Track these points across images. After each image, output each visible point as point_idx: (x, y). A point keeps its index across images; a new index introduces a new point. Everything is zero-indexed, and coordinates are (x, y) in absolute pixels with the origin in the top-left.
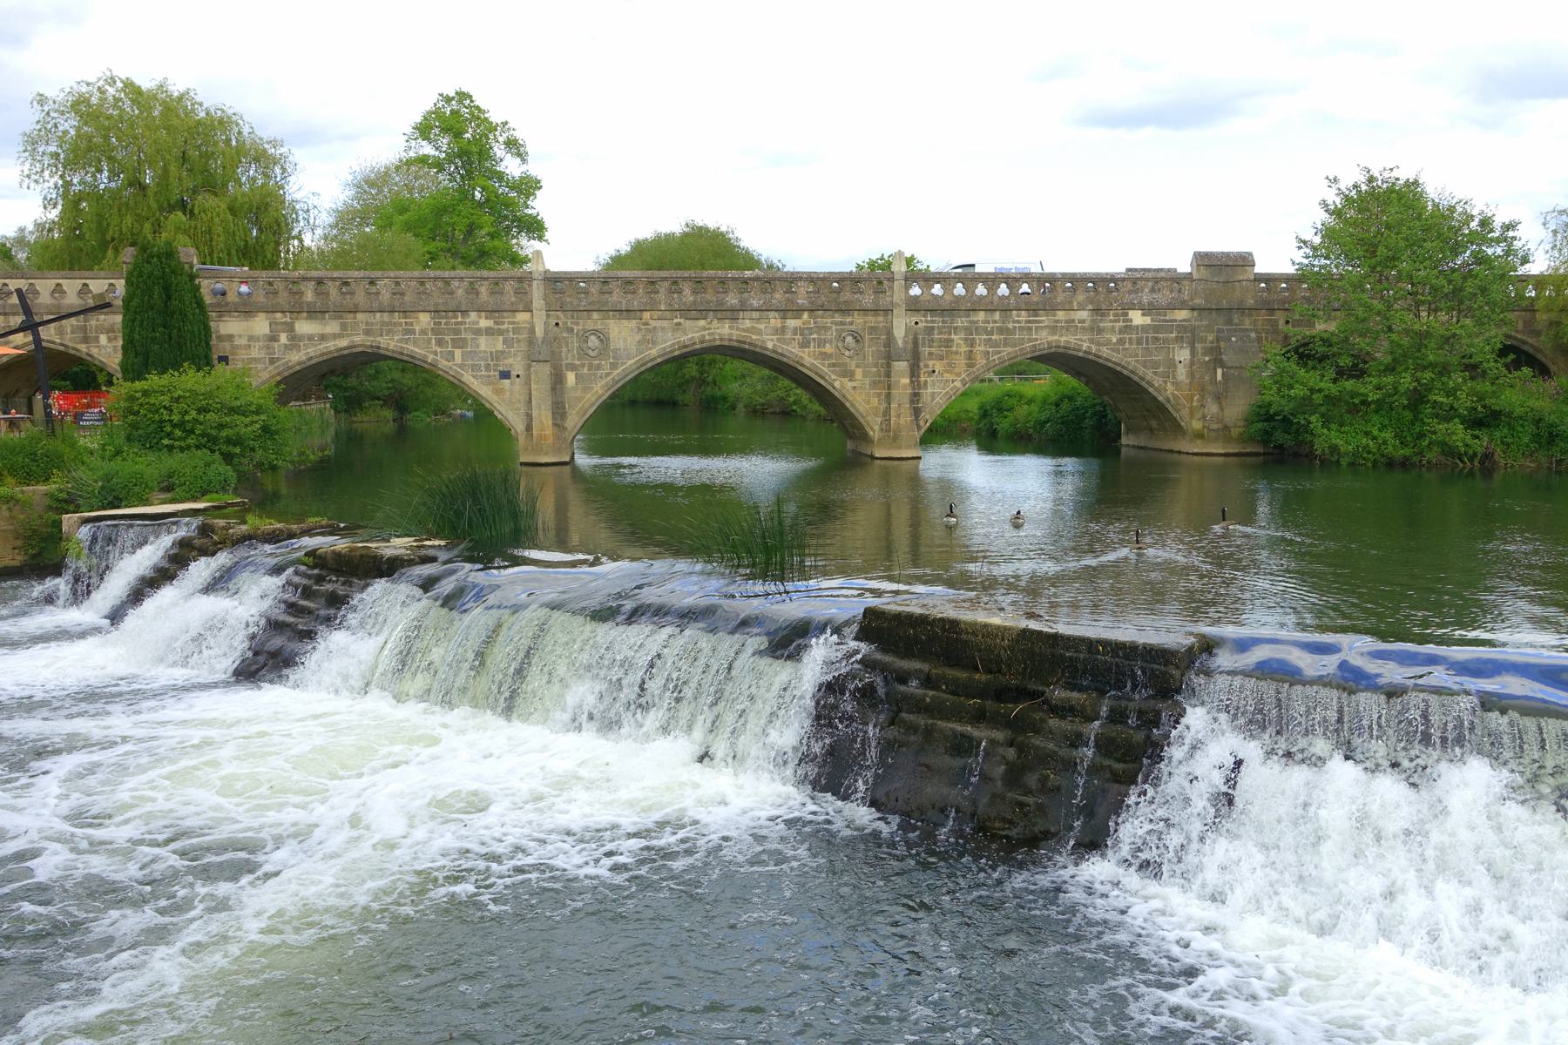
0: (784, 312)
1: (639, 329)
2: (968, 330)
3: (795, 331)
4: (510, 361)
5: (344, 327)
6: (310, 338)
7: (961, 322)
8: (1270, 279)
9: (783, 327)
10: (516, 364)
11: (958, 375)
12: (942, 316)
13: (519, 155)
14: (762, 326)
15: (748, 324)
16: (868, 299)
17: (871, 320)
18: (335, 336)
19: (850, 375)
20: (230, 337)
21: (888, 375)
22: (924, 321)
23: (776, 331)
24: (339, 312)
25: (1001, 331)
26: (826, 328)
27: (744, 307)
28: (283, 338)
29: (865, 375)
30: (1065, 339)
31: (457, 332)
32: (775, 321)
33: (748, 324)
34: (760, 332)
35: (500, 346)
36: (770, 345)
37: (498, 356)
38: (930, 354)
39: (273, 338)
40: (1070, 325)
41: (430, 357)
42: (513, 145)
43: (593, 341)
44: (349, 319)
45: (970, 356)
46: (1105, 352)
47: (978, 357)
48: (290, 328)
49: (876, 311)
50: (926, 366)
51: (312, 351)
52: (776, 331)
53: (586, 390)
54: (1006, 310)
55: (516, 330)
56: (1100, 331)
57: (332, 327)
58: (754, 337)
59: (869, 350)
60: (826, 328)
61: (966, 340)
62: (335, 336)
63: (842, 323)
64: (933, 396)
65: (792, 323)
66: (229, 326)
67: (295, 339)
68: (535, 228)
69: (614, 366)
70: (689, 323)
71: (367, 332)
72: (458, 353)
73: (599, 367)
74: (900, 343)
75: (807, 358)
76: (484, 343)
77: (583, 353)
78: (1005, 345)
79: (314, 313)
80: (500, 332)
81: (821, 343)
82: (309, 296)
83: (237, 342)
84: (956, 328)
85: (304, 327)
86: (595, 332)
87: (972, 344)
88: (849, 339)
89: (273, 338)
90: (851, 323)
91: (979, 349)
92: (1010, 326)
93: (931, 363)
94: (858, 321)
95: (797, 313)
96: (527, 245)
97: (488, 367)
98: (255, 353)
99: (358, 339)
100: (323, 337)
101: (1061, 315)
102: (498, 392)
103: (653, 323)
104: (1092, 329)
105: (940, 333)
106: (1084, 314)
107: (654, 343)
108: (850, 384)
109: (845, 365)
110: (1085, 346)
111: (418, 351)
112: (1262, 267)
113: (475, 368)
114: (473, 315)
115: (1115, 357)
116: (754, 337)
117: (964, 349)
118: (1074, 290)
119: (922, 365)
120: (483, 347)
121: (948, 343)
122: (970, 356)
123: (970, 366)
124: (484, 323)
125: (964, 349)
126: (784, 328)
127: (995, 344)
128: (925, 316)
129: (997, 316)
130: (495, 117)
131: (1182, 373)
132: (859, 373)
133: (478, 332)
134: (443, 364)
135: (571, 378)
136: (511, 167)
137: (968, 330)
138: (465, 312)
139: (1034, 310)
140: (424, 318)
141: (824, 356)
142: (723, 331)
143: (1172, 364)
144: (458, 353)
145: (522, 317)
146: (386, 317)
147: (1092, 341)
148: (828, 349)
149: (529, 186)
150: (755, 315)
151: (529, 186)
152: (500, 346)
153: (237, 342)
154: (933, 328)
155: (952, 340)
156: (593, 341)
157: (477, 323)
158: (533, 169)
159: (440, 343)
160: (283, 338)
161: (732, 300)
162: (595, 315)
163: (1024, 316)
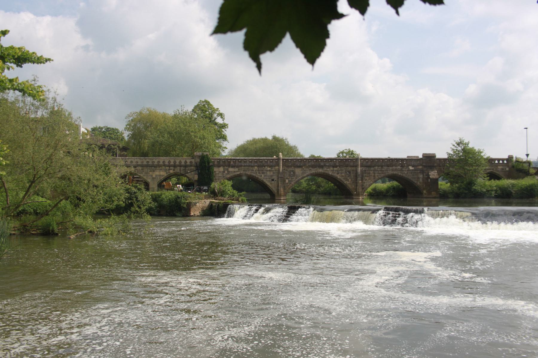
0: (334, 167)
2: (374, 171)
3: (336, 171)
5: (239, 169)
6: (232, 172)
7: (372, 169)
8: (440, 160)
10: (275, 178)
13: (222, 118)
14: (329, 170)
15: (326, 169)
16: (352, 164)
17: (353, 168)
19: (348, 180)
20: (215, 172)
21: (356, 180)
22: (364, 169)
23: (331, 171)
24: (238, 167)
25: (381, 171)
26: (343, 170)
27: (325, 166)
28: (226, 172)
30: (395, 172)
31: (263, 171)
32: (332, 169)
33: (326, 169)
34: (328, 171)
36: (330, 174)
37: (272, 176)
39: (224, 172)
40: (396, 170)
41: (257, 176)
42: (221, 115)
43: (292, 173)
44: (240, 168)
45: (374, 176)
46: (404, 175)
48: (228, 170)
49: (353, 166)
51: (232, 175)
52: (331, 171)
53: (291, 184)
54: (382, 166)
55: (275, 170)
57: (236, 169)
59: (352, 175)
60: (343, 170)
64: (366, 185)
65: (335, 169)
66: (215, 169)
67: (229, 172)
68: (224, 138)
69: (296, 178)
70: (313, 169)
71: (244, 171)
72: (263, 175)
73: (293, 178)
74: (359, 173)
75: (339, 176)
76: (268, 173)
77: (290, 176)
79: (233, 167)
80: (272, 171)
81: (342, 173)
82: (232, 163)
83: (217, 173)
85: (231, 169)
86: (293, 171)
87: (375, 173)
89: (224, 172)
91: (376, 175)
94: (349, 169)
95: (336, 167)
96: (225, 144)
97: (269, 178)
98: (220, 175)
100: (234, 172)
101: (394, 168)
102: (271, 184)
103: (305, 169)
106: (399, 167)
107: (305, 173)
108: (348, 183)
110: (400, 174)
111: (254, 175)
112: (438, 157)
113: (266, 179)
114: (266, 167)
115: (406, 177)
117: (373, 175)
118: (397, 161)
120: (268, 174)
121: (370, 173)
122: (374, 176)
123: (374, 178)
124: (269, 169)
126: (333, 170)
127: (380, 174)
129: (380, 167)
130: (215, 106)
131: (421, 180)
133: (267, 171)
134: (260, 178)
135: (287, 181)
136: (219, 120)
137: (374, 171)
138: (265, 166)
139: (388, 166)
140: (256, 168)
141: (343, 176)
142: (320, 170)
143: (419, 178)
144: (263, 175)
145: (277, 167)
146: (248, 167)
148: (343, 174)
149: (224, 126)
150: (327, 167)
151: (224, 126)
152: (272, 174)
153: (217, 173)
155: (370, 173)
158: (226, 122)
159: (259, 173)
160: (226, 172)
161: (322, 164)
162: (292, 167)
163: (386, 168)
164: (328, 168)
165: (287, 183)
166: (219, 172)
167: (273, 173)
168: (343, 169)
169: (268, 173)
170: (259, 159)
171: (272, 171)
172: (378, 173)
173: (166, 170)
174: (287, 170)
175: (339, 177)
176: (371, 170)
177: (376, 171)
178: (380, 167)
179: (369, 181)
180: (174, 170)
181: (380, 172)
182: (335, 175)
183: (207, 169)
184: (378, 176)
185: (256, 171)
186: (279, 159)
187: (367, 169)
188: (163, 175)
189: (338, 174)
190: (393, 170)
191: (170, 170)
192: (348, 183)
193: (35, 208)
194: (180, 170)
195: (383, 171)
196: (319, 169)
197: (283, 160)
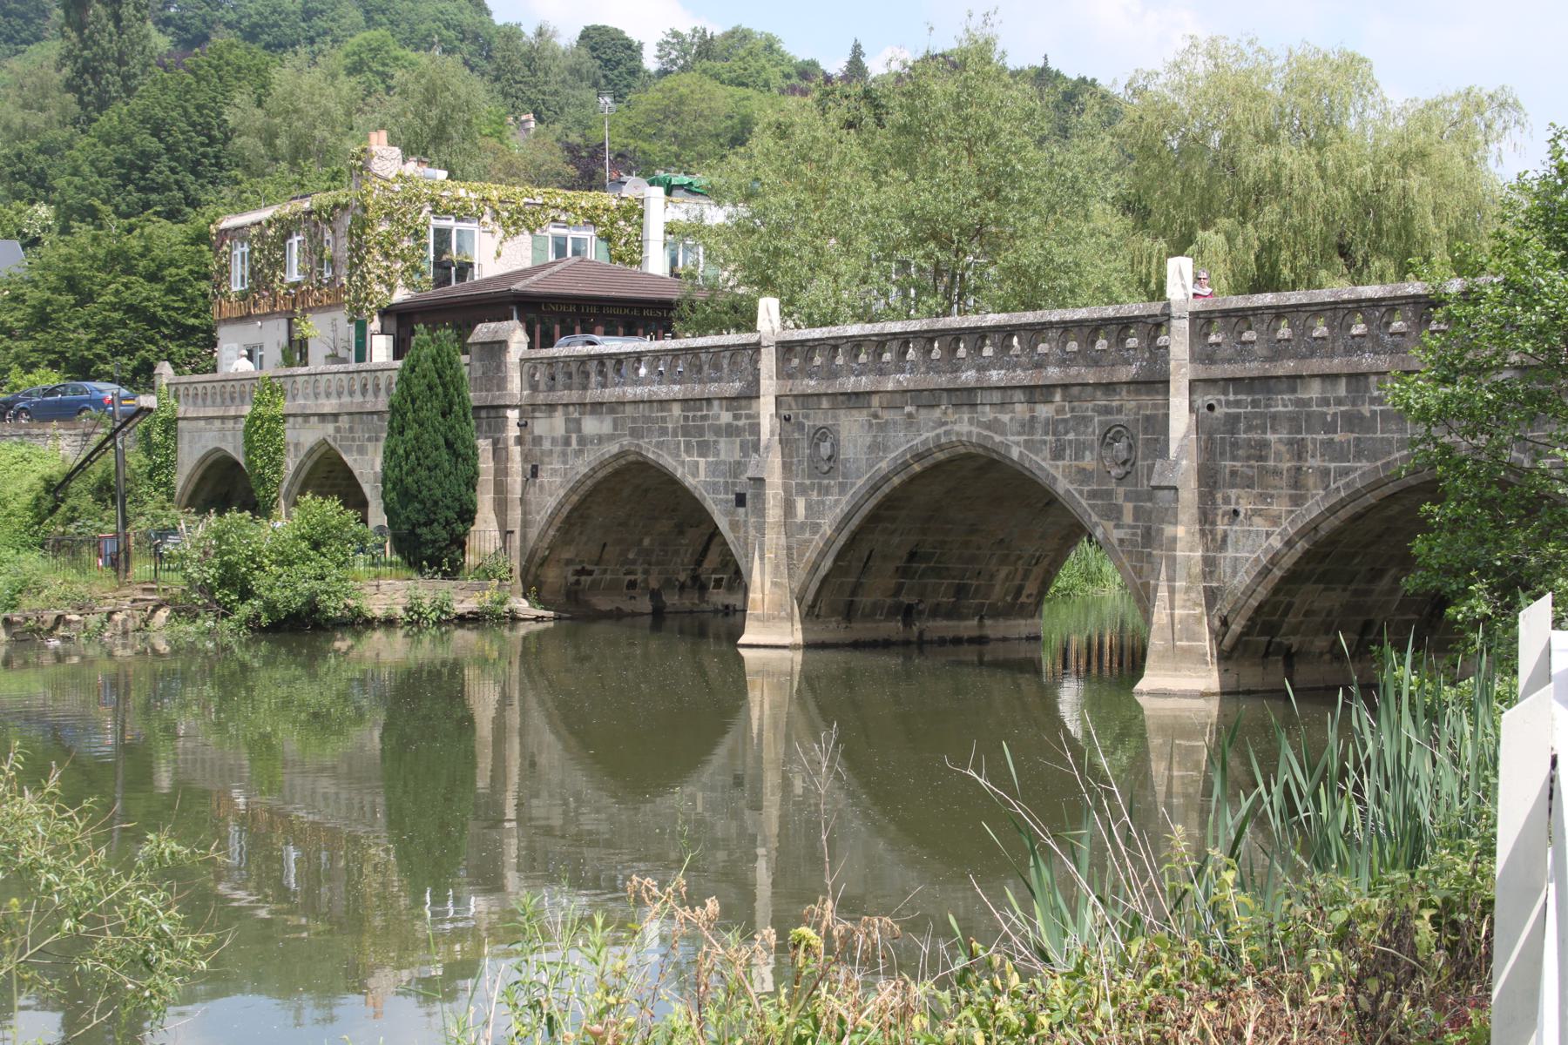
1: (871, 425)
2: (1295, 422)
7: (1282, 404)
9: (1033, 418)
12: (1250, 391)
14: (1005, 418)
15: (988, 414)
25: (1353, 421)
26: (1085, 420)
36: (1015, 453)
38: (1233, 473)
47: (1311, 481)
50: (1227, 500)
58: (998, 438)
60: (1085, 420)
61: (1290, 443)
62: (611, 438)
63: (1107, 410)
65: (1044, 411)
78: (1359, 455)
84: (1274, 417)
85: (591, 425)
90: (1120, 410)
92: (1366, 410)
93: (1233, 493)
105: (1249, 429)
107: (886, 449)
109: (1109, 494)
116: (998, 438)
119: (1219, 496)
120: (723, 457)
127: (1338, 452)
128: (1225, 393)
129: (1342, 389)
133: (718, 431)
141: (1083, 475)
144: (702, 461)
148: (1089, 461)
150: (996, 397)
152: (737, 456)
154: (1237, 417)
155: (1264, 444)
157: (718, 417)
165: (802, 526)
174: (801, 427)
178: (1342, 389)
179: (1260, 524)
181: (1338, 437)
184: (1325, 473)
187: (1244, 403)
189: (1057, 454)
197: (786, 349)
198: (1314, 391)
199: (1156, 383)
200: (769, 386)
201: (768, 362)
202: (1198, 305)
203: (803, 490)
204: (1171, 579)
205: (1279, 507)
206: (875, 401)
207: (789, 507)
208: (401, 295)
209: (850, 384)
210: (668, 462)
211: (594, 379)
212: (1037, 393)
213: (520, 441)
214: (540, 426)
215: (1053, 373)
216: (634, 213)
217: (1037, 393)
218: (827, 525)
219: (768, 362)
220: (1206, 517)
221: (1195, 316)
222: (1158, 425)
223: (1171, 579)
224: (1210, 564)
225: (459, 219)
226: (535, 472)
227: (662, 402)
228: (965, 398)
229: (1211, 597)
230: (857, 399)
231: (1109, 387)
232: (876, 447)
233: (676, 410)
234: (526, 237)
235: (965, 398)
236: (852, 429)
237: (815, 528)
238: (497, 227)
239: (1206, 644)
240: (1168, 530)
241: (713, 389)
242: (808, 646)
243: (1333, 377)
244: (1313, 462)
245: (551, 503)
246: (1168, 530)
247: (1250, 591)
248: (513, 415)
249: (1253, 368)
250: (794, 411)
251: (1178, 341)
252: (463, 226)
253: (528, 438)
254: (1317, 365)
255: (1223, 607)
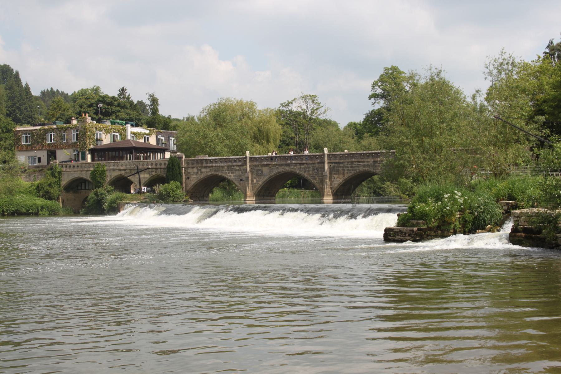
2: (343, 167)
4: (242, 177)
5: (210, 170)
7: (341, 165)
11: (341, 178)
15: (292, 167)
17: (321, 165)
18: (209, 172)
19: (315, 179)
25: (351, 167)
26: (310, 168)
28: (199, 172)
29: (319, 179)
30: (367, 169)
31: (232, 170)
32: (298, 166)
34: (295, 169)
35: (240, 174)
36: (297, 172)
37: (240, 176)
39: (197, 173)
40: (368, 166)
41: (227, 177)
48: (200, 170)
53: (258, 183)
56: (376, 166)
57: (208, 170)
60: (310, 168)
65: (302, 166)
67: (201, 172)
70: (280, 167)
71: (215, 171)
80: (241, 170)
81: (309, 171)
85: (203, 170)
86: (260, 170)
87: (344, 170)
88: (316, 170)
89: (197, 173)
97: (238, 178)
99: (213, 172)
100: (206, 172)
102: (240, 184)
103: (272, 167)
104: (374, 166)
108: (315, 181)
110: (372, 170)
117: (342, 172)
121: (338, 170)
123: (344, 176)
124: (238, 168)
125: (342, 172)
126: (300, 168)
129: (350, 163)
132: (317, 179)
133: (236, 170)
137: (343, 167)
141: (310, 174)
144: (232, 175)
147: (374, 169)
148: (310, 172)
150: (294, 165)
152: (240, 174)
155: (339, 170)
156: (260, 172)
160: (199, 172)
164: (295, 166)
165: (255, 183)
166: (193, 173)
167: (242, 172)
168: (310, 166)
169: (237, 172)
170: (228, 158)
171: (241, 170)
172: (348, 170)
173: (149, 173)
174: (255, 169)
175: (306, 176)
176: (340, 167)
177: (346, 167)
178: (350, 163)
179: (338, 179)
180: (156, 172)
181: (350, 169)
182: (302, 173)
183: (171, 170)
185: (226, 171)
186: (246, 158)
187: (336, 165)
188: (147, 178)
189: (305, 172)
190: (364, 166)
191: (152, 172)
192: (315, 182)
193: (28, 209)
194: (161, 172)
195: (354, 167)
196: (285, 167)
197: (251, 158)
198: (346, 164)
199: (324, 163)
200: (248, 163)
201: (248, 160)
202: (328, 153)
203: (255, 178)
204: (327, 186)
205: (341, 176)
206: (270, 166)
207: (252, 181)
208: (92, 147)
209: (265, 163)
210: (224, 175)
211: (204, 163)
212: (300, 164)
213: (185, 173)
214: (190, 170)
215: (304, 161)
216: (125, 130)
217: (300, 164)
218: (260, 183)
219: (248, 160)
220: (330, 179)
221: (328, 155)
222: (324, 167)
223: (327, 186)
224: (331, 184)
225: (99, 131)
226: (188, 178)
227: (222, 166)
228: (288, 165)
229: (331, 188)
230: (267, 165)
231: (314, 163)
232: (270, 172)
233: (226, 167)
234: (109, 135)
235: (288, 165)
236: (265, 170)
237: (258, 183)
238: (104, 133)
239: (331, 194)
240: (326, 180)
241: (235, 164)
242: (256, 200)
243: (348, 162)
244: (346, 172)
245: (193, 183)
246: (326, 180)
247: (337, 187)
248: (183, 169)
249: (337, 161)
250: (253, 167)
251: (326, 158)
252: (100, 132)
253: (186, 172)
254: (346, 160)
255: (333, 189)
